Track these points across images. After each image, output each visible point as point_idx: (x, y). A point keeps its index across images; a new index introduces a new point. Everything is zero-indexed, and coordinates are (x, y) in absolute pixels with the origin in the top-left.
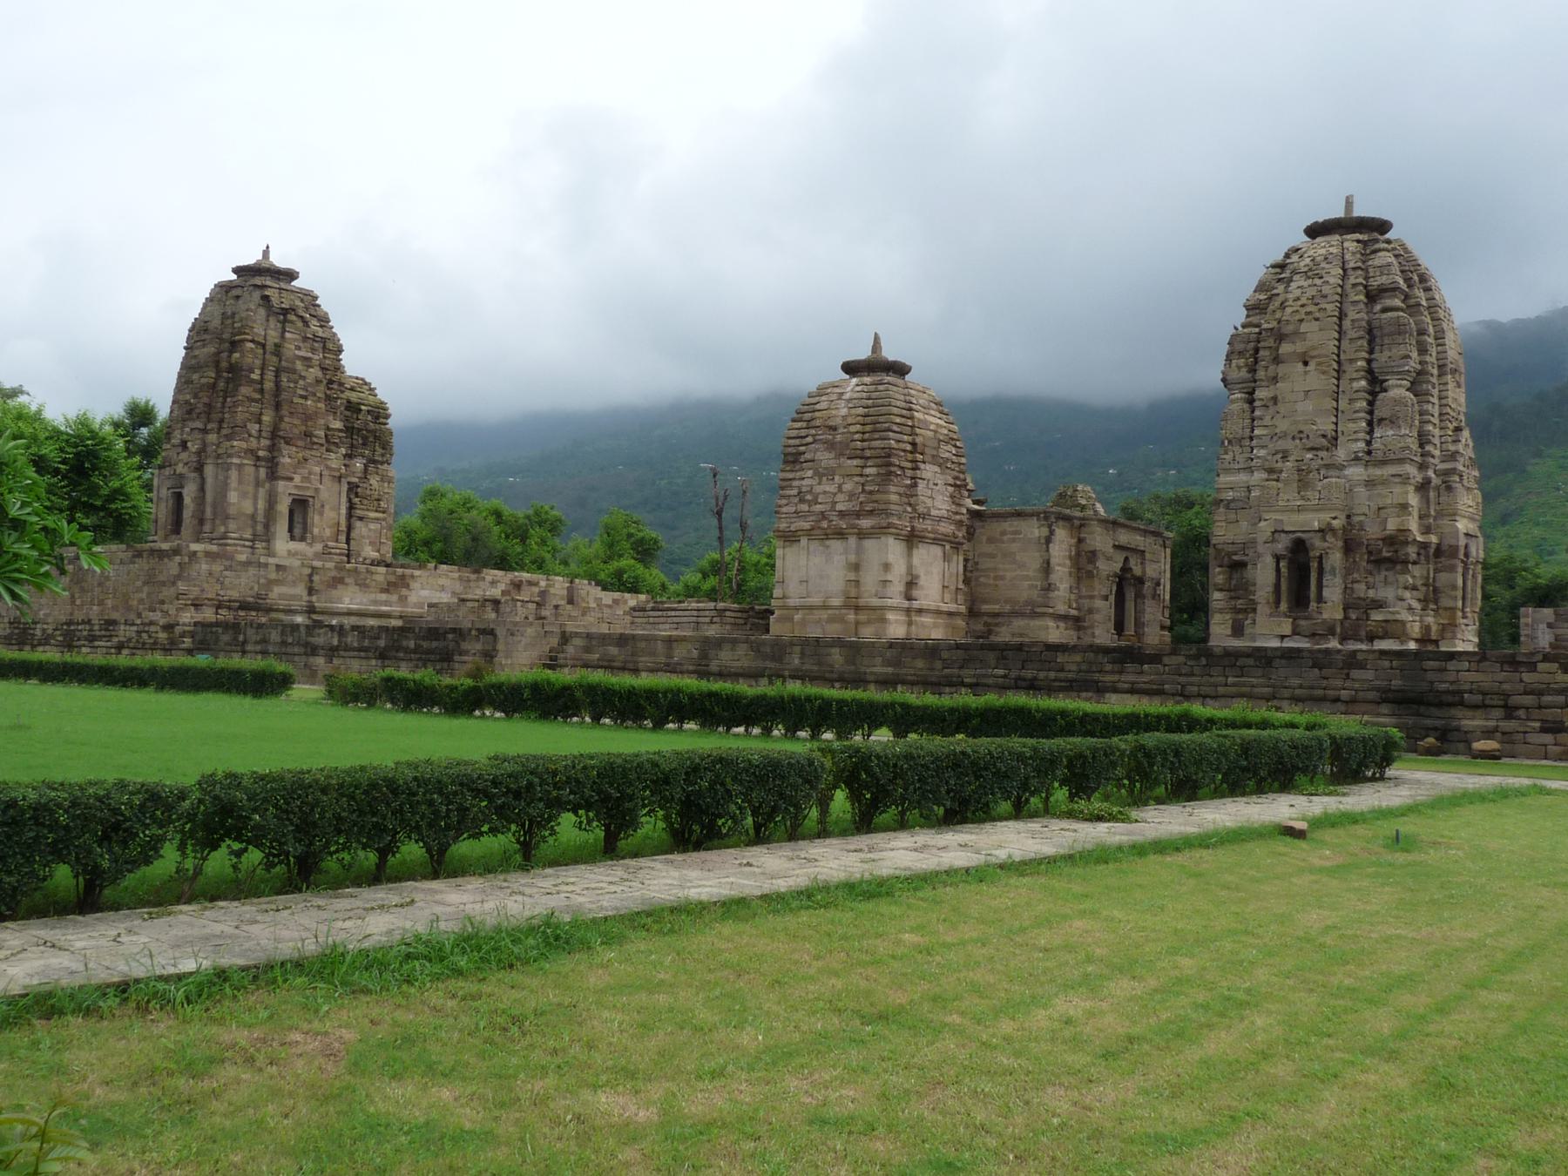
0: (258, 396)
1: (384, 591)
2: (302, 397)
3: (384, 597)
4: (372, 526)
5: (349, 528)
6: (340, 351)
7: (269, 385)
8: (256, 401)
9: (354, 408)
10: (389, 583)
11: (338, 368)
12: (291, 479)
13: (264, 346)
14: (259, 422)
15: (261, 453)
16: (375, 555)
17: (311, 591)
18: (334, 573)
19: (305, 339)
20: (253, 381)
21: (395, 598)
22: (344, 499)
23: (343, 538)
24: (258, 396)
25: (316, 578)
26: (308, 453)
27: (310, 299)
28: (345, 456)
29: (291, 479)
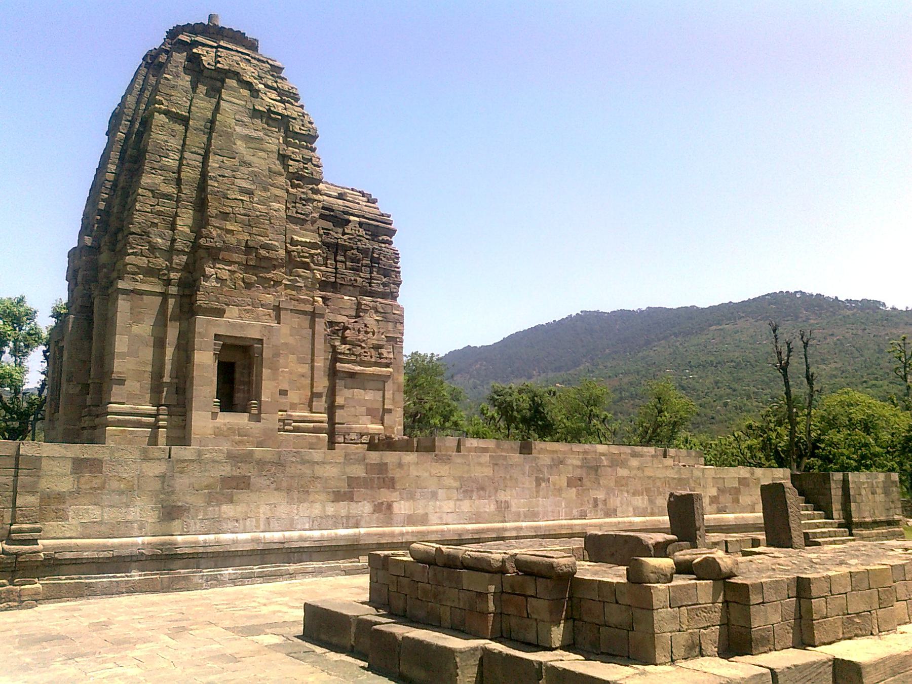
0: (171, 190)
1: (338, 497)
2: (243, 191)
3: (343, 508)
5: (332, 392)
7: (190, 174)
8: (168, 196)
9: (337, 219)
10: (352, 481)
13: (184, 121)
14: (173, 227)
16: (376, 428)
17: (171, 512)
18: (227, 470)
19: (255, 113)
21: (365, 508)
22: (320, 345)
23: (321, 404)
24: (171, 190)
25: (181, 482)
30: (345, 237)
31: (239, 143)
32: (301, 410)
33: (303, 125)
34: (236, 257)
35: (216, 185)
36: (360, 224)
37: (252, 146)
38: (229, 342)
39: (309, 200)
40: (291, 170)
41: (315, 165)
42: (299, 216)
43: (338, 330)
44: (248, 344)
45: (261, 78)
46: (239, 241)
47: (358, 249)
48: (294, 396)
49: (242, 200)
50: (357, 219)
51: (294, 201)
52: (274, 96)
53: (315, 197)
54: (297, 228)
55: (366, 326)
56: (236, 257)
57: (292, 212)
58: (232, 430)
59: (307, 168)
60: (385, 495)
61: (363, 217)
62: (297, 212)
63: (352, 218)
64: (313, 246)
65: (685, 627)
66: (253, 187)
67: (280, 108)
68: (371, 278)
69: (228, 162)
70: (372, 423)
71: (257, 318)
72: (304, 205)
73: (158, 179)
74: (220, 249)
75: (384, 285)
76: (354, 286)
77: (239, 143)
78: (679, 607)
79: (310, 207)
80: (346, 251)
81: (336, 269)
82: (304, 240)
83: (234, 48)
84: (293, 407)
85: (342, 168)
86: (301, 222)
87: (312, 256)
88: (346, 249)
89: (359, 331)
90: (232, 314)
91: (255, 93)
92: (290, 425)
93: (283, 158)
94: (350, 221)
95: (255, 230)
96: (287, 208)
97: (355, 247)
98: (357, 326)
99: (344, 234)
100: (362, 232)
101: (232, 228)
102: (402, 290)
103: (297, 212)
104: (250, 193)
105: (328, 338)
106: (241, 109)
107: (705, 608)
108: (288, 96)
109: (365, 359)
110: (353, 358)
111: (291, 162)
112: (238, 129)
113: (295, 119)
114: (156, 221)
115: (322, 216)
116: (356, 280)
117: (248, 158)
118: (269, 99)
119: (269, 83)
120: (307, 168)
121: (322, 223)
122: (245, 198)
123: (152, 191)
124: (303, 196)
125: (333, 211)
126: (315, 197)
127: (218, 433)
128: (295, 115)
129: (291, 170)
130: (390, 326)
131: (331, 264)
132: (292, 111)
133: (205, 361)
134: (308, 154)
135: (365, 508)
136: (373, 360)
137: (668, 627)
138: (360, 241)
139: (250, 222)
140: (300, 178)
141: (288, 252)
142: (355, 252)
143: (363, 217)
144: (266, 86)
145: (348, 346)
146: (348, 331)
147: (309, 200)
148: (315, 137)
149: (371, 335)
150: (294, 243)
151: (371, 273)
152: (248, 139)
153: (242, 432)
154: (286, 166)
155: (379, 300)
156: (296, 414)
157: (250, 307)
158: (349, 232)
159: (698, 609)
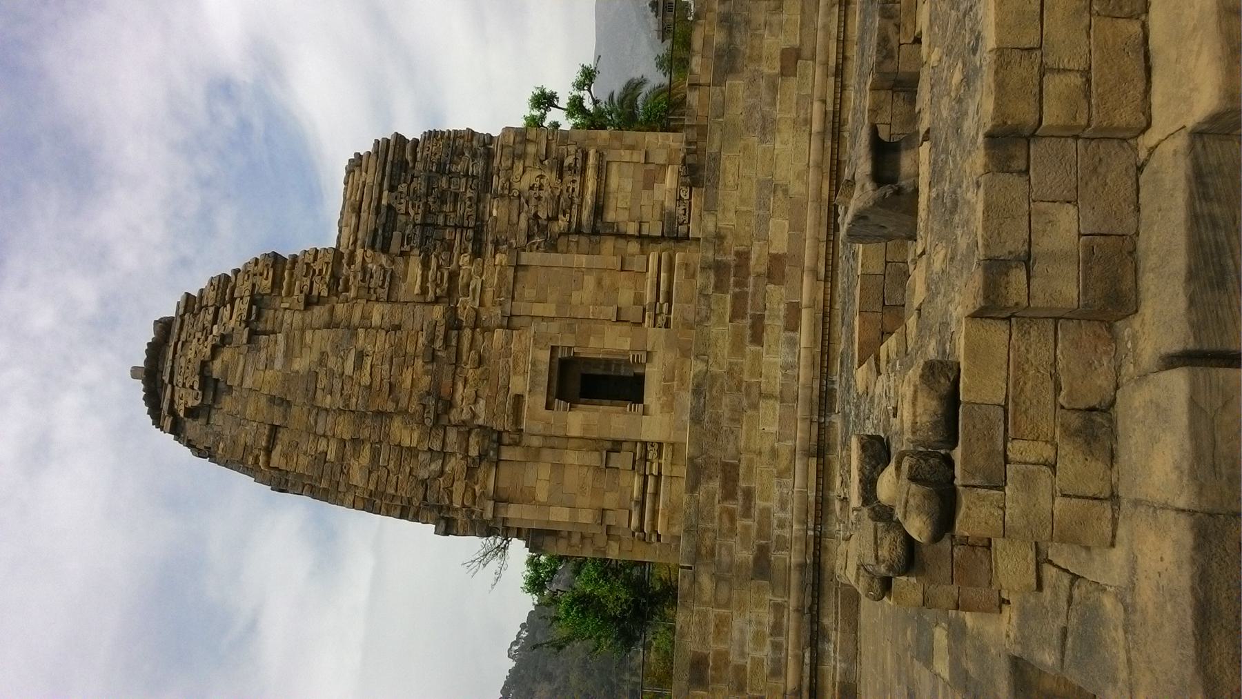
2: (359, 365)
4: (614, 182)
6: (276, 259)
8: (375, 454)
11: (308, 263)
12: (519, 398)
14: (413, 452)
15: (474, 452)
16: (670, 179)
20: (341, 458)
21: (777, 298)
24: (366, 451)
26: (469, 356)
27: (190, 304)
28: (477, 254)
29: (519, 398)
30: (412, 212)
31: (296, 367)
32: (644, 286)
33: (261, 274)
34: (447, 381)
35: (354, 400)
36: (392, 189)
37: (297, 348)
38: (554, 390)
39: (364, 268)
40: (325, 293)
41: (315, 259)
42: (387, 283)
43: (537, 226)
44: (556, 366)
45: (204, 328)
46: (426, 373)
47: (427, 195)
48: (626, 298)
49: (372, 366)
50: (385, 193)
51: (368, 293)
52: (227, 313)
53: (359, 259)
54: (403, 286)
55: (532, 188)
56: (447, 381)
57: (383, 293)
58: (667, 390)
59: (321, 271)
60: (758, 263)
61: (381, 185)
62: (382, 287)
63: (384, 202)
64: (425, 265)
65: (1048, 452)
66: (353, 351)
67: (242, 306)
68: (466, 175)
69: (323, 382)
70: (663, 181)
71: (526, 351)
72: (371, 277)
73: (355, 465)
74: (439, 398)
75: (474, 156)
76: (479, 200)
77: (296, 367)
78: (1007, 461)
79: (372, 266)
80: (430, 212)
81: (456, 227)
82: (419, 279)
83: (169, 363)
84: (639, 299)
85: (318, 222)
86: (392, 280)
87: (439, 267)
88: (427, 211)
89: (539, 198)
90: (518, 384)
91: (225, 340)
92: (661, 306)
93: (309, 303)
94: (389, 207)
95: (410, 349)
96: (377, 300)
97: (424, 200)
98: (533, 202)
99: (407, 213)
100: (403, 188)
101: (409, 382)
102: (480, 129)
103: (382, 287)
104: (361, 356)
105: (552, 247)
106: (250, 361)
107: (1016, 384)
108: (223, 285)
109: (577, 190)
110: (575, 211)
111: (315, 293)
112: (278, 364)
113: (254, 285)
114: (408, 470)
115: (385, 249)
116: (470, 198)
117: (315, 356)
118: (232, 319)
119: (210, 318)
120: (321, 271)
121: (395, 247)
122: (368, 361)
123: (370, 472)
124: (359, 277)
125: (376, 230)
126: (359, 259)
127: (669, 406)
128: (248, 285)
129: (325, 293)
130: (531, 149)
131: (451, 233)
132: (244, 289)
133: (578, 420)
134: (300, 269)
135: (777, 298)
136: (578, 179)
137: (1044, 502)
138: (415, 191)
139: (399, 358)
140: (335, 277)
141: (437, 300)
142: (431, 199)
143: (381, 185)
144: (214, 322)
145: (561, 216)
146: (540, 214)
147: (364, 268)
148: (275, 255)
149: (544, 181)
150: (424, 291)
151: (457, 174)
152: (289, 354)
153: (668, 378)
154: (320, 301)
155: (495, 165)
156: (649, 297)
157: (511, 360)
158: (403, 208)
159: (1016, 404)
